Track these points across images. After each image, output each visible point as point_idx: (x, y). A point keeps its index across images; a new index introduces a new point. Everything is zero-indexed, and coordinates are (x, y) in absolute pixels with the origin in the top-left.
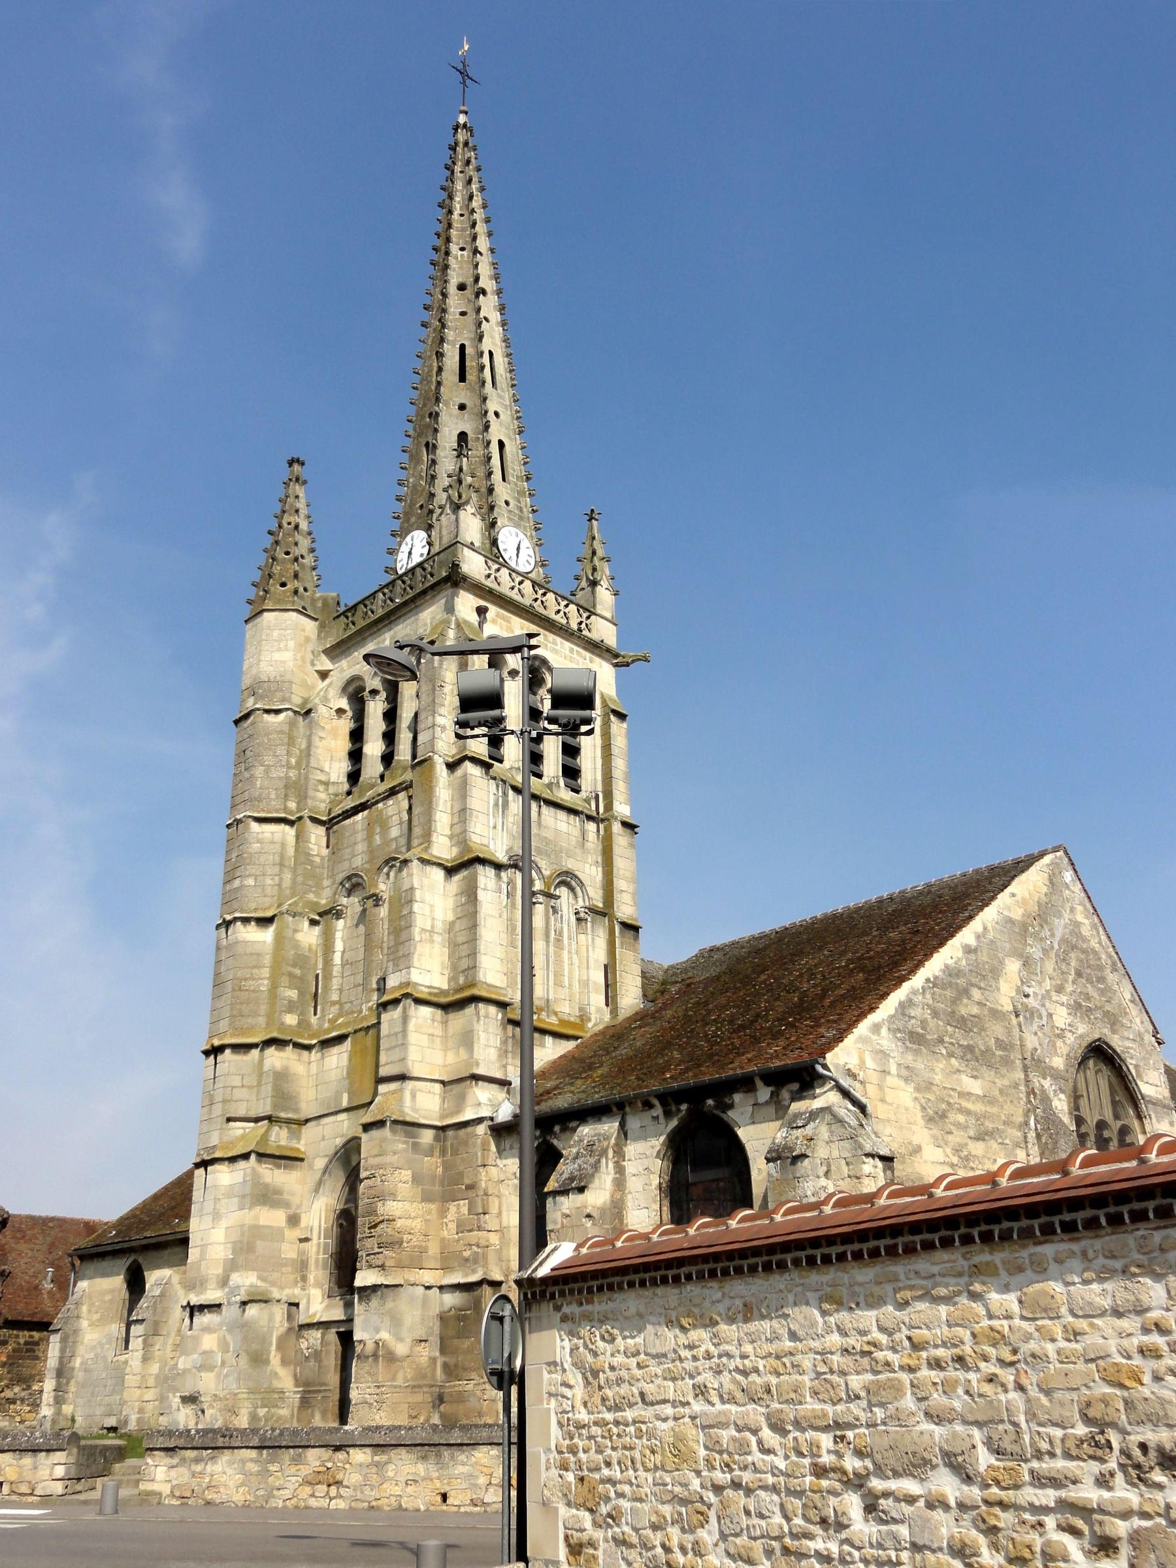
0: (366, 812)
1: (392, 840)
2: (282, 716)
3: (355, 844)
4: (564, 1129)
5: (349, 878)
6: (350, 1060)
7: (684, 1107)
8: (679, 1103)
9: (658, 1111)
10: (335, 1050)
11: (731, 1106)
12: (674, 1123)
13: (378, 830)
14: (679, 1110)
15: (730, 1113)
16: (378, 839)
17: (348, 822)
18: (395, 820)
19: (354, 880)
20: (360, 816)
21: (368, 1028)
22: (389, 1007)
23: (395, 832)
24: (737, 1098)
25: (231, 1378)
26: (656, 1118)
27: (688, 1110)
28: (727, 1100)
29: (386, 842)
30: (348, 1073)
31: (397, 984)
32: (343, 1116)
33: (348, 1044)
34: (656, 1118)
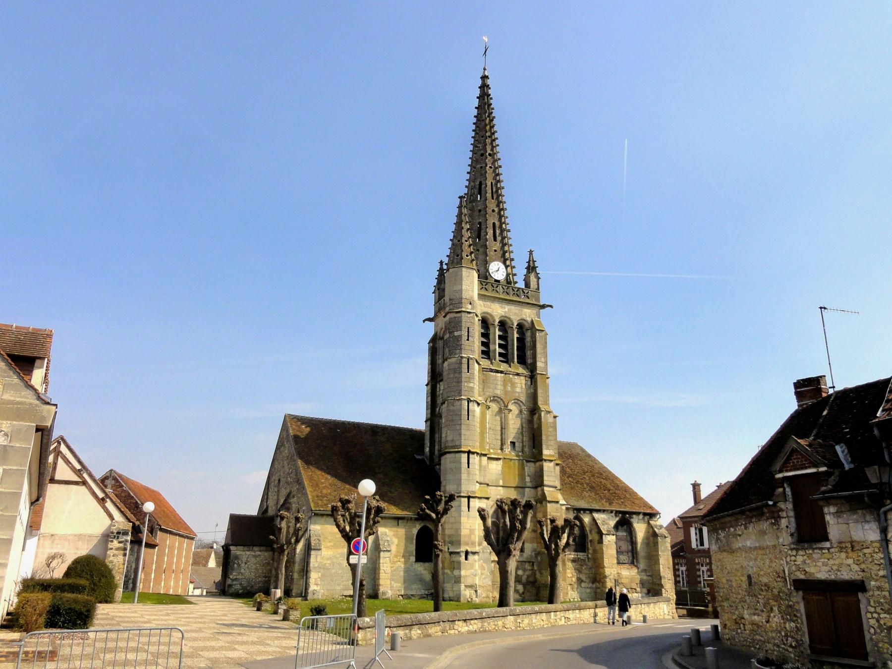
0: (503, 375)
1: (517, 392)
2: (472, 315)
3: (497, 384)
4: (584, 513)
5: (494, 397)
9: (613, 514)
10: (495, 462)
11: (633, 518)
12: (618, 519)
16: (509, 388)
18: (519, 385)
19: (495, 398)
21: (512, 459)
23: (518, 390)
24: (634, 516)
25: (487, 579)
26: (612, 516)
27: (622, 516)
32: (501, 488)
33: (501, 462)
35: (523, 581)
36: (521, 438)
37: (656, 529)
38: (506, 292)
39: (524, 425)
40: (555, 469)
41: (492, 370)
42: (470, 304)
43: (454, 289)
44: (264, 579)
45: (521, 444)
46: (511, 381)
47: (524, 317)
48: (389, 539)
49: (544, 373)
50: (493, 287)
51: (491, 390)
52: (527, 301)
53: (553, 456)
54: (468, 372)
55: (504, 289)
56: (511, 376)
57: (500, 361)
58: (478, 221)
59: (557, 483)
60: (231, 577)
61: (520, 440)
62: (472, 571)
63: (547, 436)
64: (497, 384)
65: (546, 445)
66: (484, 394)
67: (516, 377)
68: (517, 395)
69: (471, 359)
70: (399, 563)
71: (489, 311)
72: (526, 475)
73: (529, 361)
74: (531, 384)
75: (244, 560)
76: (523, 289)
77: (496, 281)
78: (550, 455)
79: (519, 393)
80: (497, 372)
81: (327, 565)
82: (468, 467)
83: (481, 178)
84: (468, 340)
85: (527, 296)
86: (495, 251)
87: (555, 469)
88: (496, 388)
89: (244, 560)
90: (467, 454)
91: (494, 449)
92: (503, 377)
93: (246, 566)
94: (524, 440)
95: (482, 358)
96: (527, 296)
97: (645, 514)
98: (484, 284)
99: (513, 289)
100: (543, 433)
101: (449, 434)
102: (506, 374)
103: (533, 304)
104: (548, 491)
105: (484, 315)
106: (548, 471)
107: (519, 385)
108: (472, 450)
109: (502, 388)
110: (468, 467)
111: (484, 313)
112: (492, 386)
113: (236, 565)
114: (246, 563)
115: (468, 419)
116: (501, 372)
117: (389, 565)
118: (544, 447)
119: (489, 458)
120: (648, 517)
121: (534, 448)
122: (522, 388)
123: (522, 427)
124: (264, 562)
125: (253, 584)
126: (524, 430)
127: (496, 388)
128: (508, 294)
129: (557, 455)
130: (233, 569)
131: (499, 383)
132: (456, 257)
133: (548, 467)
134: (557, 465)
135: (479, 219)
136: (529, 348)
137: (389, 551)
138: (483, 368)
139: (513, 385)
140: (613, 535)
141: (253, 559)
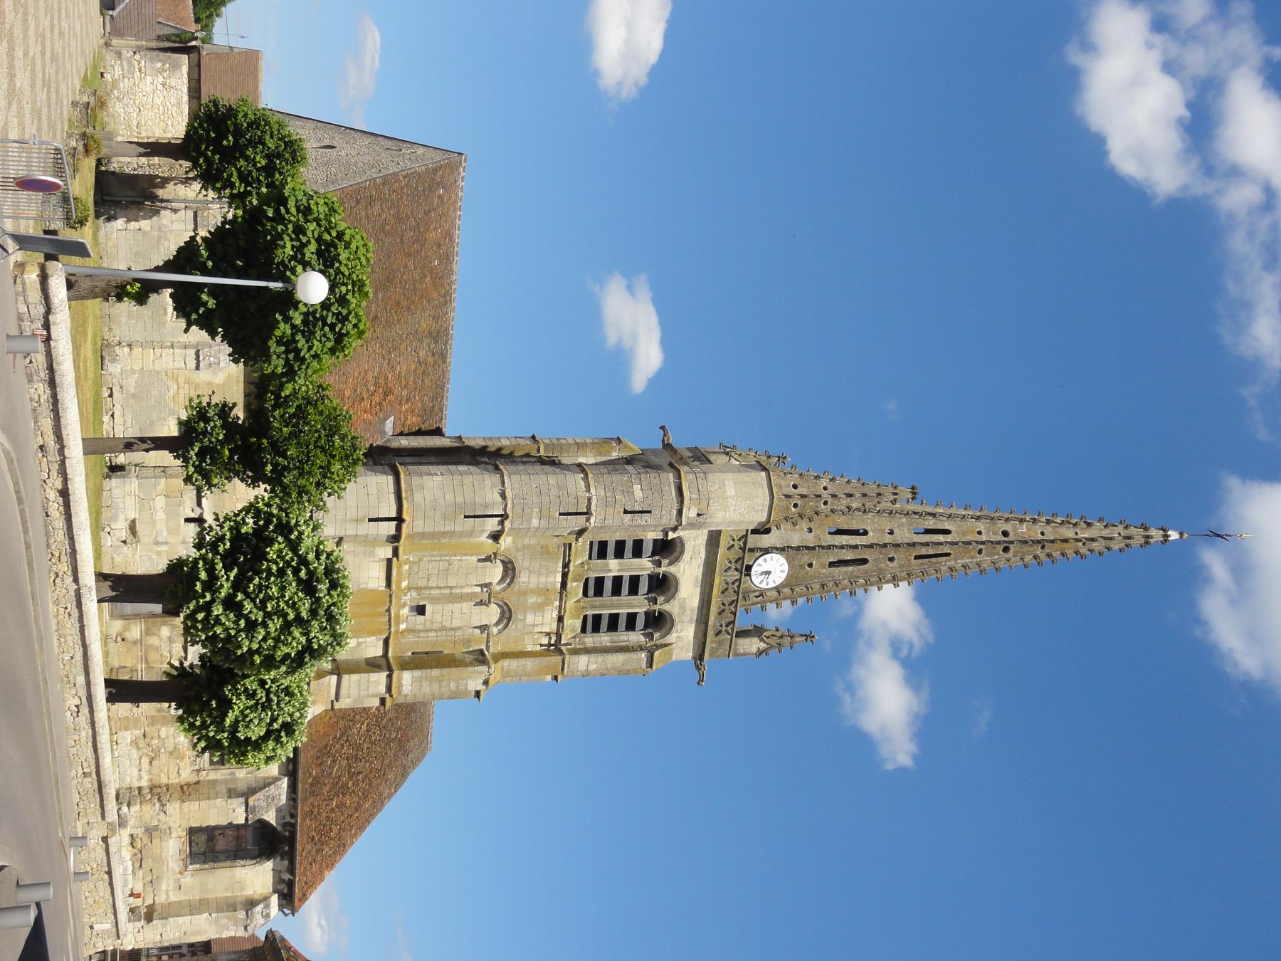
1: (525, 616)
5: (514, 569)
6: (372, 591)
7: (287, 834)
8: (290, 832)
10: (383, 575)
11: (282, 859)
12: (279, 829)
13: (539, 600)
14: (285, 831)
15: (279, 858)
16: (532, 600)
17: (560, 565)
18: (539, 620)
19: (510, 572)
20: (559, 579)
22: (389, 679)
24: (286, 862)
27: (285, 836)
28: (286, 857)
29: (525, 611)
30: (364, 589)
31: (404, 682)
34: (284, 818)
35: (148, 638)
36: (435, 626)
37: (261, 906)
38: (727, 589)
39: (459, 633)
40: (374, 696)
41: (566, 565)
42: (699, 515)
43: (727, 482)
44: (135, 123)
45: (421, 627)
46: (548, 602)
47: (678, 627)
48: (222, 364)
49: (566, 670)
50: (736, 562)
51: (526, 564)
52: (711, 633)
53: (400, 693)
54: (560, 514)
55: (733, 583)
56: (557, 603)
57: (587, 580)
58: (868, 529)
59: (344, 703)
60: (137, 56)
61: (428, 626)
62: (165, 533)
63: (440, 680)
64: (539, 574)
65: (421, 677)
66: (517, 550)
67: (555, 614)
68: (520, 617)
69: (588, 520)
70: (175, 386)
71: (687, 556)
72: (360, 640)
73: (590, 640)
74: (541, 645)
75: (173, 82)
76: (733, 622)
77: (749, 568)
78: (400, 685)
79: (524, 620)
80: (565, 576)
81: (166, 243)
82: (370, 520)
83: (957, 533)
84: (626, 512)
85: (720, 632)
86: (810, 565)
87: (374, 696)
88: (530, 572)
89: (173, 82)
90: (394, 514)
91: (409, 572)
92: (555, 588)
93: (160, 87)
94: (430, 634)
95: (591, 543)
96: (720, 632)
97: (291, 884)
98: (741, 543)
99: (733, 602)
100: (446, 671)
101: (435, 478)
102: (561, 593)
103: (704, 644)
104: (329, 683)
105: (679, 545)
106: (369, 682)
107: (539, 620)
108: (404, 526)
109: (533, 586)
110: (370, 520)
111: (683, 545)
112: (536, 565)
113: (159, 65)
114: (163, 85)
115: (466, 517)
116: (564, 584)
117: (171, 366)
118: (417, 673)
119: (389, 561)
120: (286, 891)
121: (413, 653)
122: (534, 625)
123: (454, 629)
124: (169, 123)
125: (125, 101)
126: (452, 633)
127: (530, 572)
128: (723, 592)
129: (401, 700)
130: (152, 60)
131: (543, 579)
132: (792, 483)
133: (377, 683)
134: (383, 701)
135: (874, 531)
136: (616, 638)
137: (198, 368)
138: (570, 545)
139: (539, 608)
140: (247, 819)
141: (173, 100)
